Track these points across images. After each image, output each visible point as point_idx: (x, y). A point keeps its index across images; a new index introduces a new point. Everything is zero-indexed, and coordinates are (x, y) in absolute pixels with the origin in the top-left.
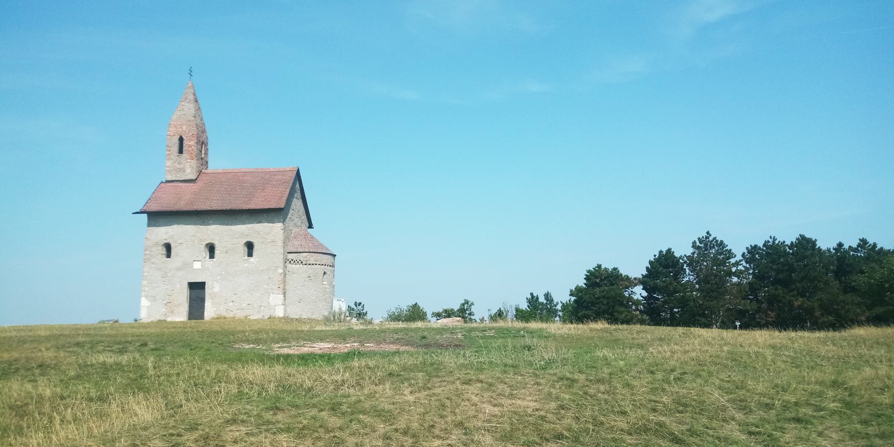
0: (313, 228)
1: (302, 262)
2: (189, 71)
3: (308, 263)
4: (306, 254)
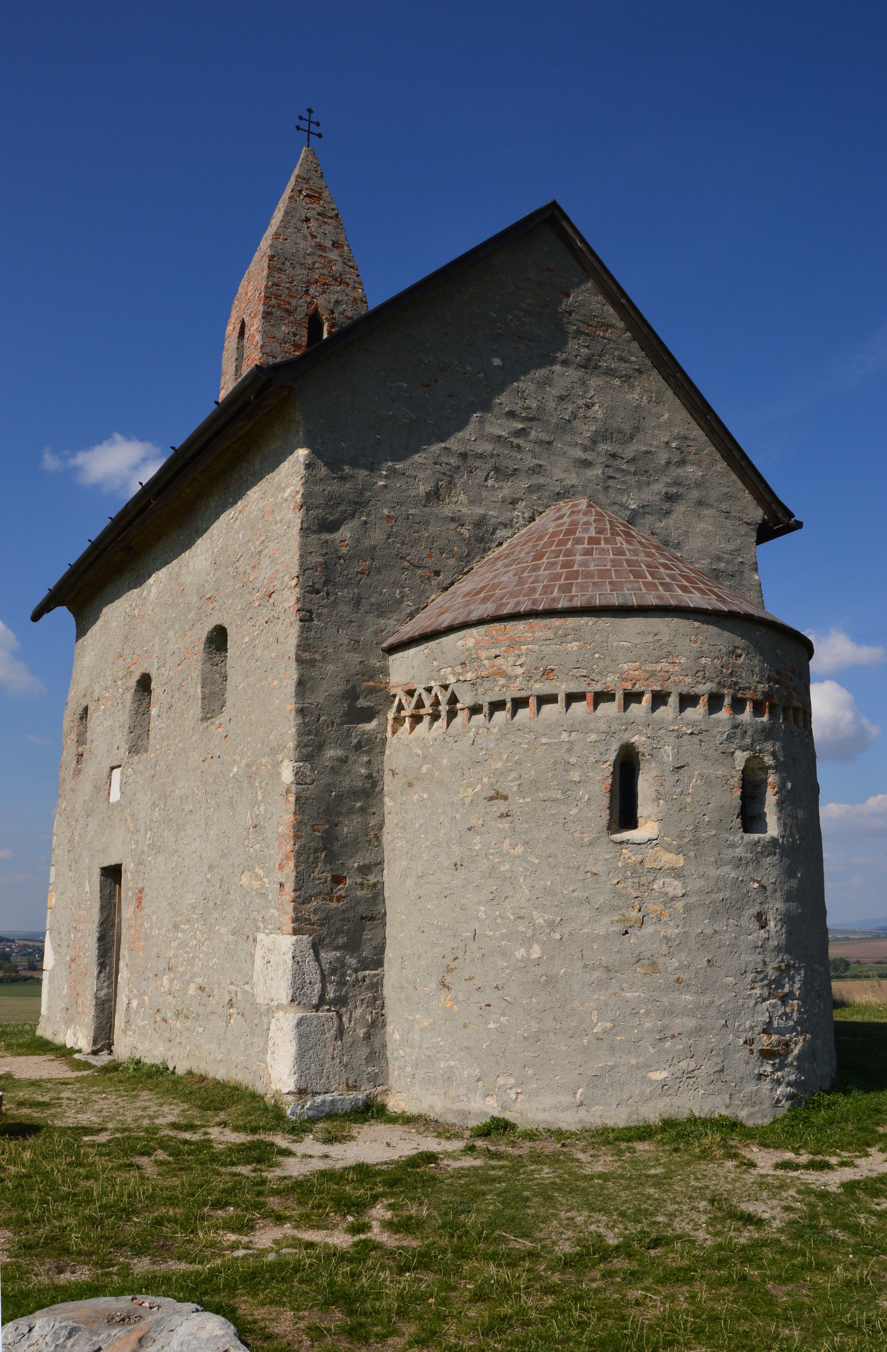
0: (799, 525)
1: (453, 700)
2: (304, 125)
3: (485, 701)
4: (469, 639)
